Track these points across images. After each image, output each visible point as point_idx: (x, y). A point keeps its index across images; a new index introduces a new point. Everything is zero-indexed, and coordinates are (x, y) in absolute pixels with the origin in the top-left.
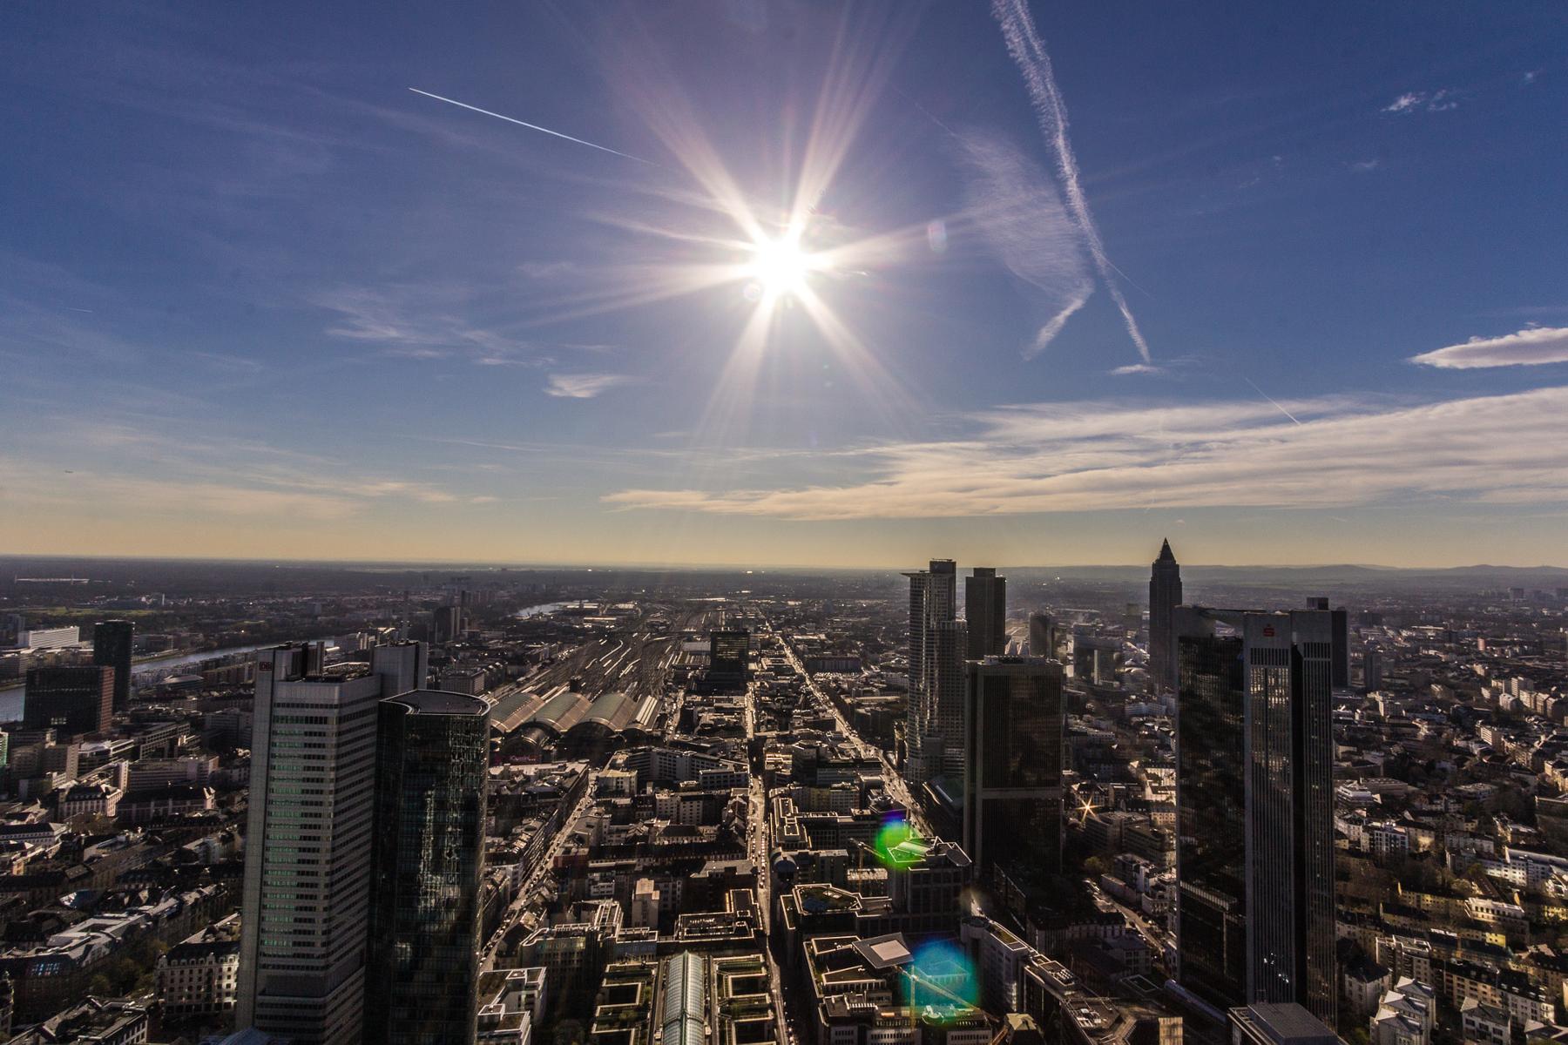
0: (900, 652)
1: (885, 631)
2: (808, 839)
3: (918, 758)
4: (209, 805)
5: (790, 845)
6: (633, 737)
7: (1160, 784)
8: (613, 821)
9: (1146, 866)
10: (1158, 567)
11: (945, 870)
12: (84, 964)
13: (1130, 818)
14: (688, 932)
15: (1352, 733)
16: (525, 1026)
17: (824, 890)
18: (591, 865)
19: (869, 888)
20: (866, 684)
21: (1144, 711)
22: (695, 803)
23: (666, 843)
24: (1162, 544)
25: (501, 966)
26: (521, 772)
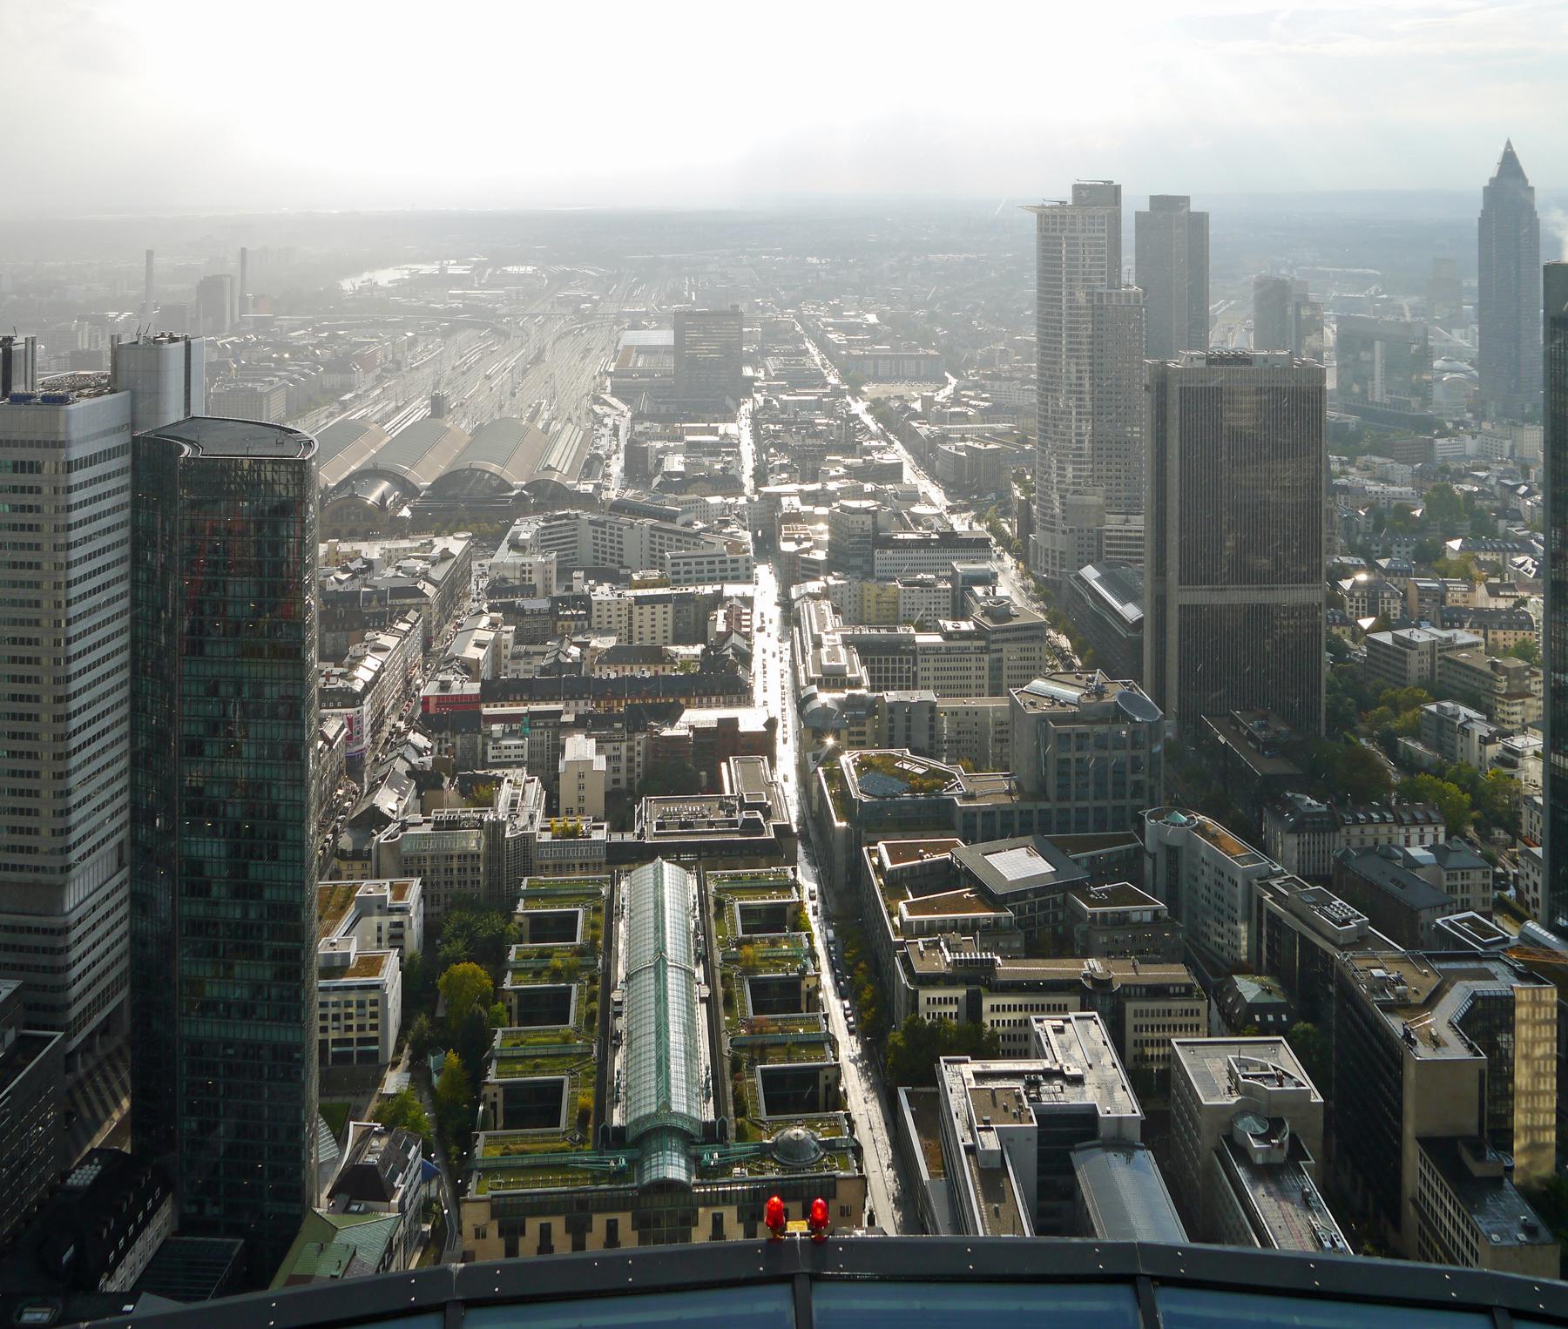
2: (862, 672)
3: (1053, 531)
5: (832, 679)
7: (1502, 579)
8: (519, 638)
13: (1449, 640)
14: (659, 826)
16: (391, 975)
17: (898, 759)
18: (486, 711)
22: (659, 608)
23: (613, 676)
25: (344, 874)
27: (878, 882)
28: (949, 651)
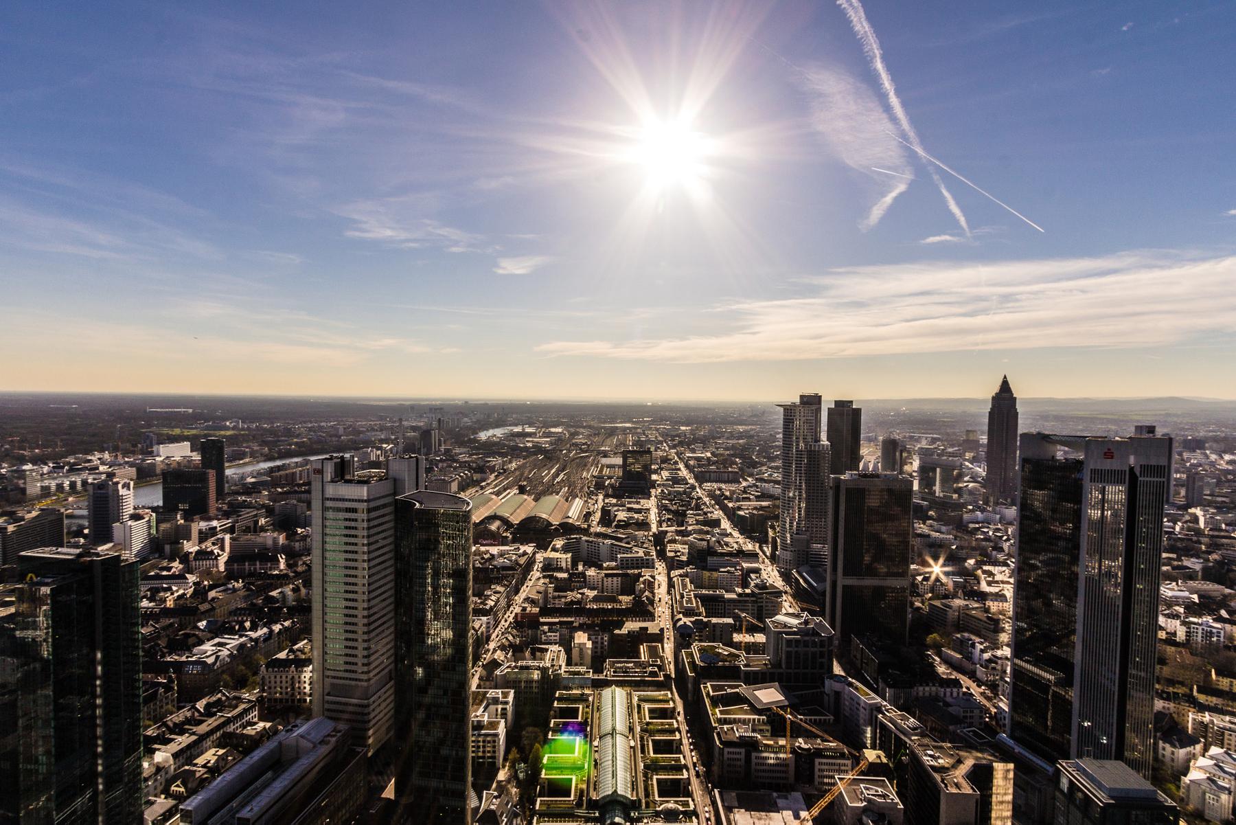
0: (771, 468)
1: (758, 451)
2: (702, 610)
4: (282, 566)
5: (688, 613)
6: (566, 529)
7: (994, 578)
8: (556, 590)
9: (981, 643)
10: (996, 399)
11: (813, 638)
12: (215, 667)
14: (614, 672)
15: (1172, 542)
16: (501, 730)
17: (716, 648)
18: (541, 620)
19: (751, 648)
20: (745, 492)
21: (979, 519)
22: (615, 579)
23: (595, 607)
24: (1002, 380)
26: (488, 551)
27: (707, 701)
28: (739, 601)
